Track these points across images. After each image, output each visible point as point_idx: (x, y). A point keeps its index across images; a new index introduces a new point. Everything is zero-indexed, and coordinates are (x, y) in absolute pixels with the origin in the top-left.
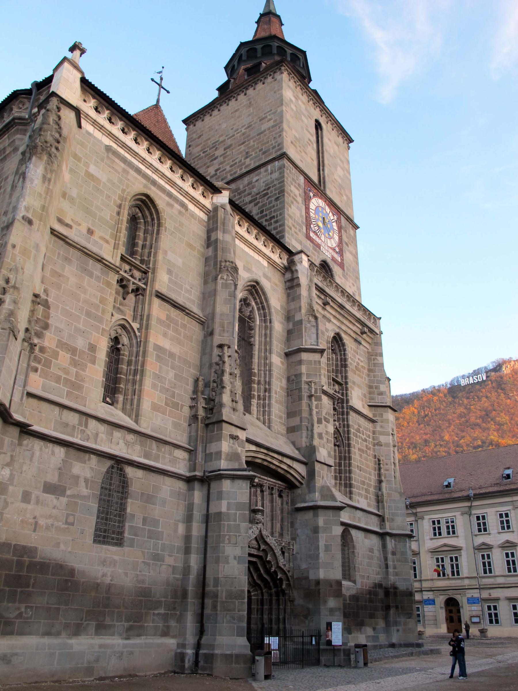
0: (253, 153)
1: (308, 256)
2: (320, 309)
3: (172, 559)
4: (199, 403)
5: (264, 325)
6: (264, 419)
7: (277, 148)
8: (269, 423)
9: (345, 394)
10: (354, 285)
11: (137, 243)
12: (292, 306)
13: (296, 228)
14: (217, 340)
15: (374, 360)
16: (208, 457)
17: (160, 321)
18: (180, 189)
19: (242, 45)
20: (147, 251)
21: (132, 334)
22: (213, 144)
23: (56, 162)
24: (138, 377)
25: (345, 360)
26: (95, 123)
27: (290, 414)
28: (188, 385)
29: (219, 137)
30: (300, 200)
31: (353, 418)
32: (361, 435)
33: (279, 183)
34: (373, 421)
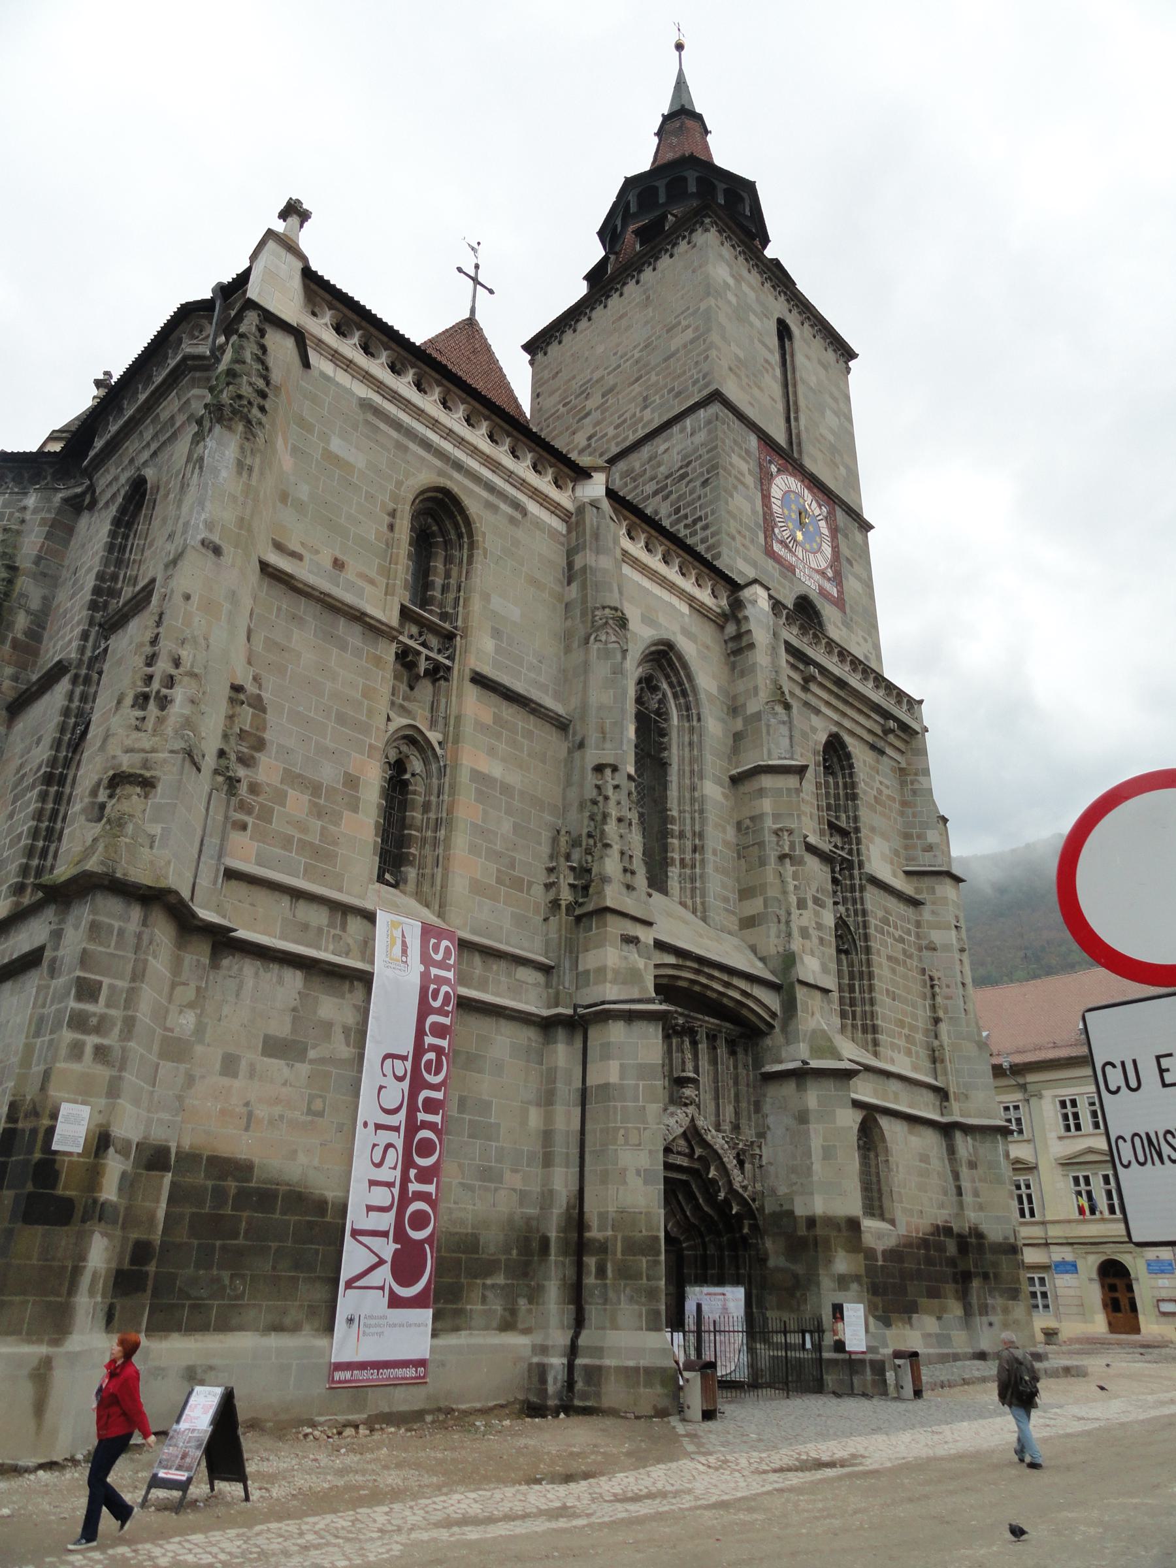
0: (657, 397)
1: (768, 589)
2: (798, 691)
3: (518, 1176)
4: (562, 876)
5: (687, 725)
6: (694, 903)
7: (702, 383)
8: (704, 911)
9: (855, 852)
10: (866, 640)
11: (433, 581)
12: (741, 686)
13: (744, 537)
14: (593, 756)
15: (912, 784)
16: (583, 979)
17: (480, 726)
18: (509, 476)
19: (630, 184)
20: (451, 596)
21: (430, 753)
22: (581, 386)
23: (261, 435)
24: (443, 832)
25: (853, 785)
26: (336, 357)
27: (746, 893)
28: (540, 844)
29: (593, 372)
30: (750, 480)
31: (873, 899)
32: (891, 930)
33: (708, 452)
34: (915, 903)
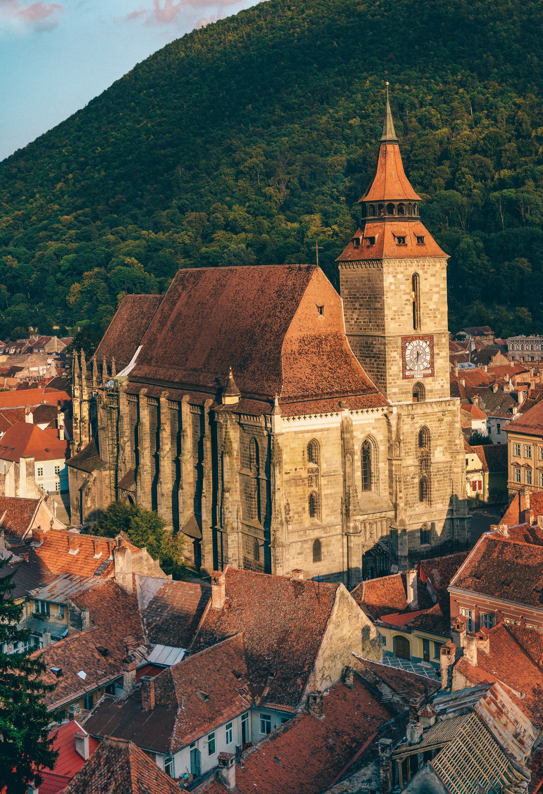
10: (442, 380)
30: (398, 357)
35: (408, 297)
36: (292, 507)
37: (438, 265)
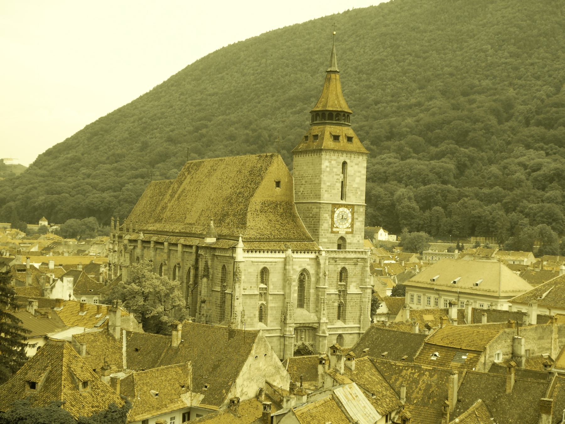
17: (271, 300)
30: (328, 218)
35: (338, 177)
36: (246, 312)
37: (361, 158)
